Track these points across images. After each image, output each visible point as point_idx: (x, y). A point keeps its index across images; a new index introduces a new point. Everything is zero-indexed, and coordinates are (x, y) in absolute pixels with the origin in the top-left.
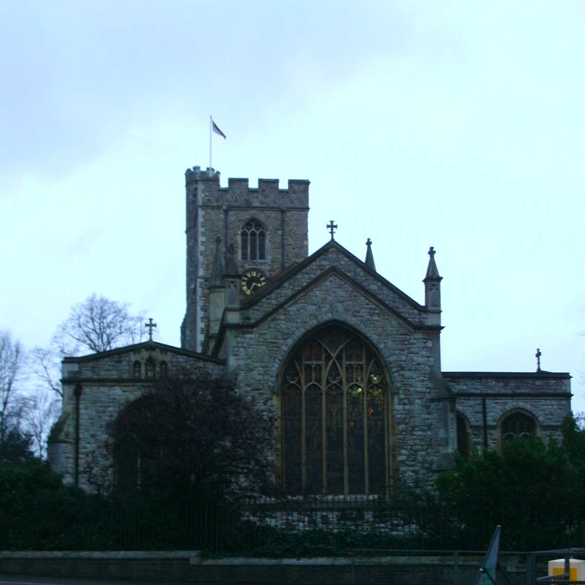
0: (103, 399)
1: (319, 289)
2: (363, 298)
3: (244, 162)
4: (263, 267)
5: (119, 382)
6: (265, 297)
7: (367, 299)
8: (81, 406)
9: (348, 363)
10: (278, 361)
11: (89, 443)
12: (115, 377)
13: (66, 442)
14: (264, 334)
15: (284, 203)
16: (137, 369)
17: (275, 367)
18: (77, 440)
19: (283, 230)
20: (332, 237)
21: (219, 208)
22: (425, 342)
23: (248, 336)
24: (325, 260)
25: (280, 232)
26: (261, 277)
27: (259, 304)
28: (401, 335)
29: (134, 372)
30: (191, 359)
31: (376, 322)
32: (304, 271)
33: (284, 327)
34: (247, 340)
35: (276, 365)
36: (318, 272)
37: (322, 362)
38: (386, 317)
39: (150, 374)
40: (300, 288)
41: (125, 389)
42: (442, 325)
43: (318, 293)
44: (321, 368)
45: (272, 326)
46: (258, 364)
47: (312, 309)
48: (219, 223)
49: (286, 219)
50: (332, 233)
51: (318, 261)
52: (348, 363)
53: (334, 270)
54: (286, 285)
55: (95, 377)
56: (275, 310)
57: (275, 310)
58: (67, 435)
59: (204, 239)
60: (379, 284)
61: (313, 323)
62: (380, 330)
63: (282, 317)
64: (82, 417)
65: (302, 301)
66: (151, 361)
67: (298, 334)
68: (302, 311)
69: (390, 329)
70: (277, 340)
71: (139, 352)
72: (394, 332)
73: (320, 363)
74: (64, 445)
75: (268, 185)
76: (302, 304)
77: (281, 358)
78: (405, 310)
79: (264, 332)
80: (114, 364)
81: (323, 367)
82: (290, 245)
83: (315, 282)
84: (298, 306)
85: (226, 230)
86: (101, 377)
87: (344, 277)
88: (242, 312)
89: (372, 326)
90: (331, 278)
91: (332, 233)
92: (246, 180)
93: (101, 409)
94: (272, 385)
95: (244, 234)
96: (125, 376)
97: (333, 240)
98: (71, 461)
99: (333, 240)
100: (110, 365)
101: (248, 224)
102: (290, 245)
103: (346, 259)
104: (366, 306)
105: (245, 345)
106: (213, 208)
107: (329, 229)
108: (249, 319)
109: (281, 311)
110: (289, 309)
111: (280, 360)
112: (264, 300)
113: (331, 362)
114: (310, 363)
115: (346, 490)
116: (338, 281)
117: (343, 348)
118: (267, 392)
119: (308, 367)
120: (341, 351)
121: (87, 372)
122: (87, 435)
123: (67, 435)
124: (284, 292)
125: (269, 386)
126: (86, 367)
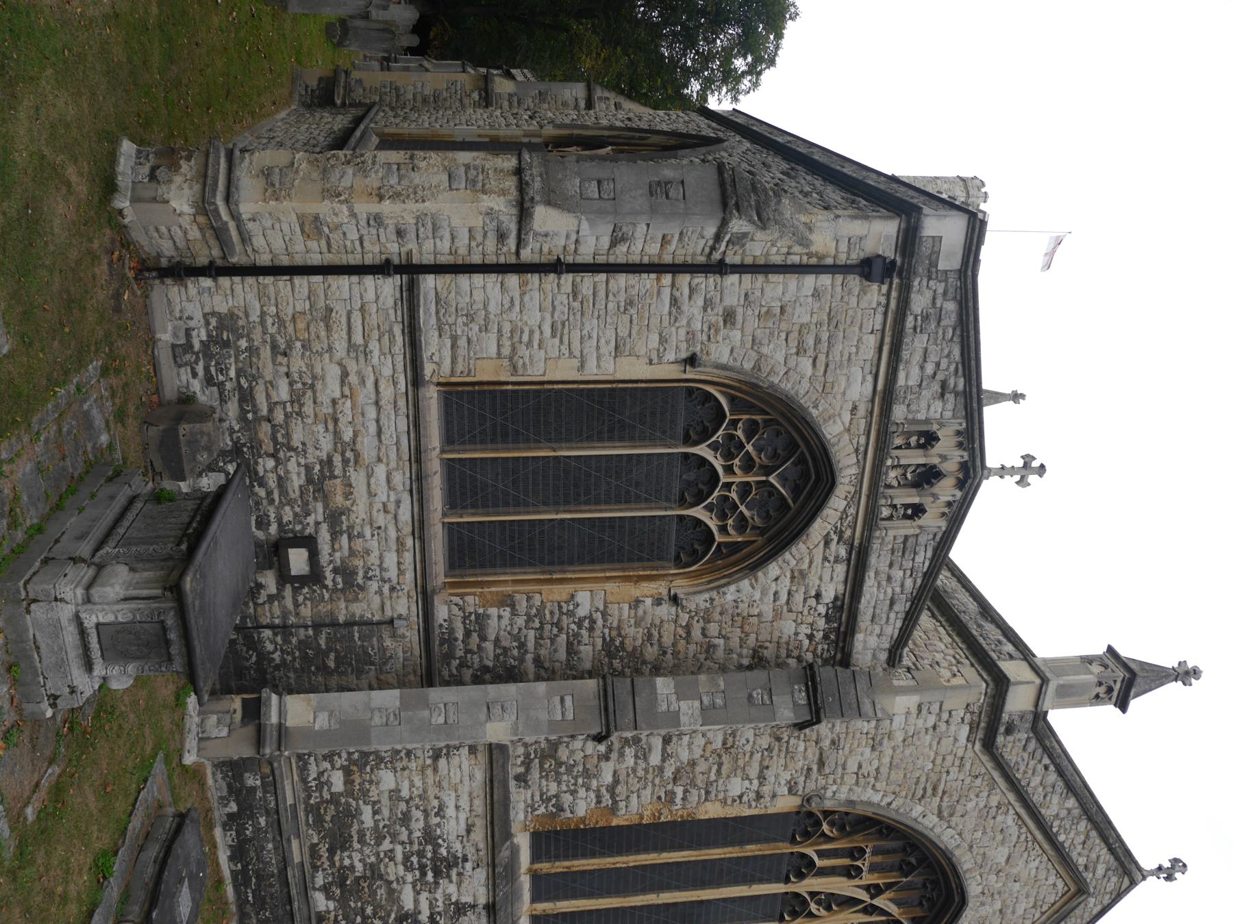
0: (838, 347)
5: (887, 397)
6: (1053, 762)
8: (826, 279)
10: (888, 800)
11: (708, 304)
12: (901, 381)
13: (718, 238)
14: (961, 766)
17: (872, 797)
18: (721, 268)
24: (1108, 870)
27: (1040, 751)
29: (908, 435)
30: (919, 581)
32: (1094, 834)
33: (970, 805)
34: (953, 728)
35: (876, 798)
36: (1082, 861)
37: (868, 879)
41: (862, 411)
44: (850, 876)
46: (886, 760)
53: (1081, 889)
54: (1071, 802)
56: (1014, 785)
57: (1014, 785)
58: (740, 239)
63: (994, 801)
64: (792, 280)
65: (1023, 836)
66: (927, 476)
67: (946, 837)
68: (999, 837)
71: (960, 445)
74: (711, 231)
76: (1014, 839)
77: (894, 806)
79: (968, 766)
80: (940, 376)
81: (857, 882)
84: (1014, 830)
88: (1031, 717)
90: (1060, 884)
93: (810, 341)
94: (829, 794)
98: (654, 249)
100: (938, 364)
105: (943, 726)
108: (1009, 731)
109: (1011, 797)
110: (1011, 812)
111: (890, 804)
112: (1046, 761)
113: (863, 895)
115: (544, 867)
117: (890, 915)
120: (883, 912)
121: (929, 294)
122: (732, 300)
123: (740, 239)
124: (1056, 799)
125: (825, 788)
126: (945, 293)
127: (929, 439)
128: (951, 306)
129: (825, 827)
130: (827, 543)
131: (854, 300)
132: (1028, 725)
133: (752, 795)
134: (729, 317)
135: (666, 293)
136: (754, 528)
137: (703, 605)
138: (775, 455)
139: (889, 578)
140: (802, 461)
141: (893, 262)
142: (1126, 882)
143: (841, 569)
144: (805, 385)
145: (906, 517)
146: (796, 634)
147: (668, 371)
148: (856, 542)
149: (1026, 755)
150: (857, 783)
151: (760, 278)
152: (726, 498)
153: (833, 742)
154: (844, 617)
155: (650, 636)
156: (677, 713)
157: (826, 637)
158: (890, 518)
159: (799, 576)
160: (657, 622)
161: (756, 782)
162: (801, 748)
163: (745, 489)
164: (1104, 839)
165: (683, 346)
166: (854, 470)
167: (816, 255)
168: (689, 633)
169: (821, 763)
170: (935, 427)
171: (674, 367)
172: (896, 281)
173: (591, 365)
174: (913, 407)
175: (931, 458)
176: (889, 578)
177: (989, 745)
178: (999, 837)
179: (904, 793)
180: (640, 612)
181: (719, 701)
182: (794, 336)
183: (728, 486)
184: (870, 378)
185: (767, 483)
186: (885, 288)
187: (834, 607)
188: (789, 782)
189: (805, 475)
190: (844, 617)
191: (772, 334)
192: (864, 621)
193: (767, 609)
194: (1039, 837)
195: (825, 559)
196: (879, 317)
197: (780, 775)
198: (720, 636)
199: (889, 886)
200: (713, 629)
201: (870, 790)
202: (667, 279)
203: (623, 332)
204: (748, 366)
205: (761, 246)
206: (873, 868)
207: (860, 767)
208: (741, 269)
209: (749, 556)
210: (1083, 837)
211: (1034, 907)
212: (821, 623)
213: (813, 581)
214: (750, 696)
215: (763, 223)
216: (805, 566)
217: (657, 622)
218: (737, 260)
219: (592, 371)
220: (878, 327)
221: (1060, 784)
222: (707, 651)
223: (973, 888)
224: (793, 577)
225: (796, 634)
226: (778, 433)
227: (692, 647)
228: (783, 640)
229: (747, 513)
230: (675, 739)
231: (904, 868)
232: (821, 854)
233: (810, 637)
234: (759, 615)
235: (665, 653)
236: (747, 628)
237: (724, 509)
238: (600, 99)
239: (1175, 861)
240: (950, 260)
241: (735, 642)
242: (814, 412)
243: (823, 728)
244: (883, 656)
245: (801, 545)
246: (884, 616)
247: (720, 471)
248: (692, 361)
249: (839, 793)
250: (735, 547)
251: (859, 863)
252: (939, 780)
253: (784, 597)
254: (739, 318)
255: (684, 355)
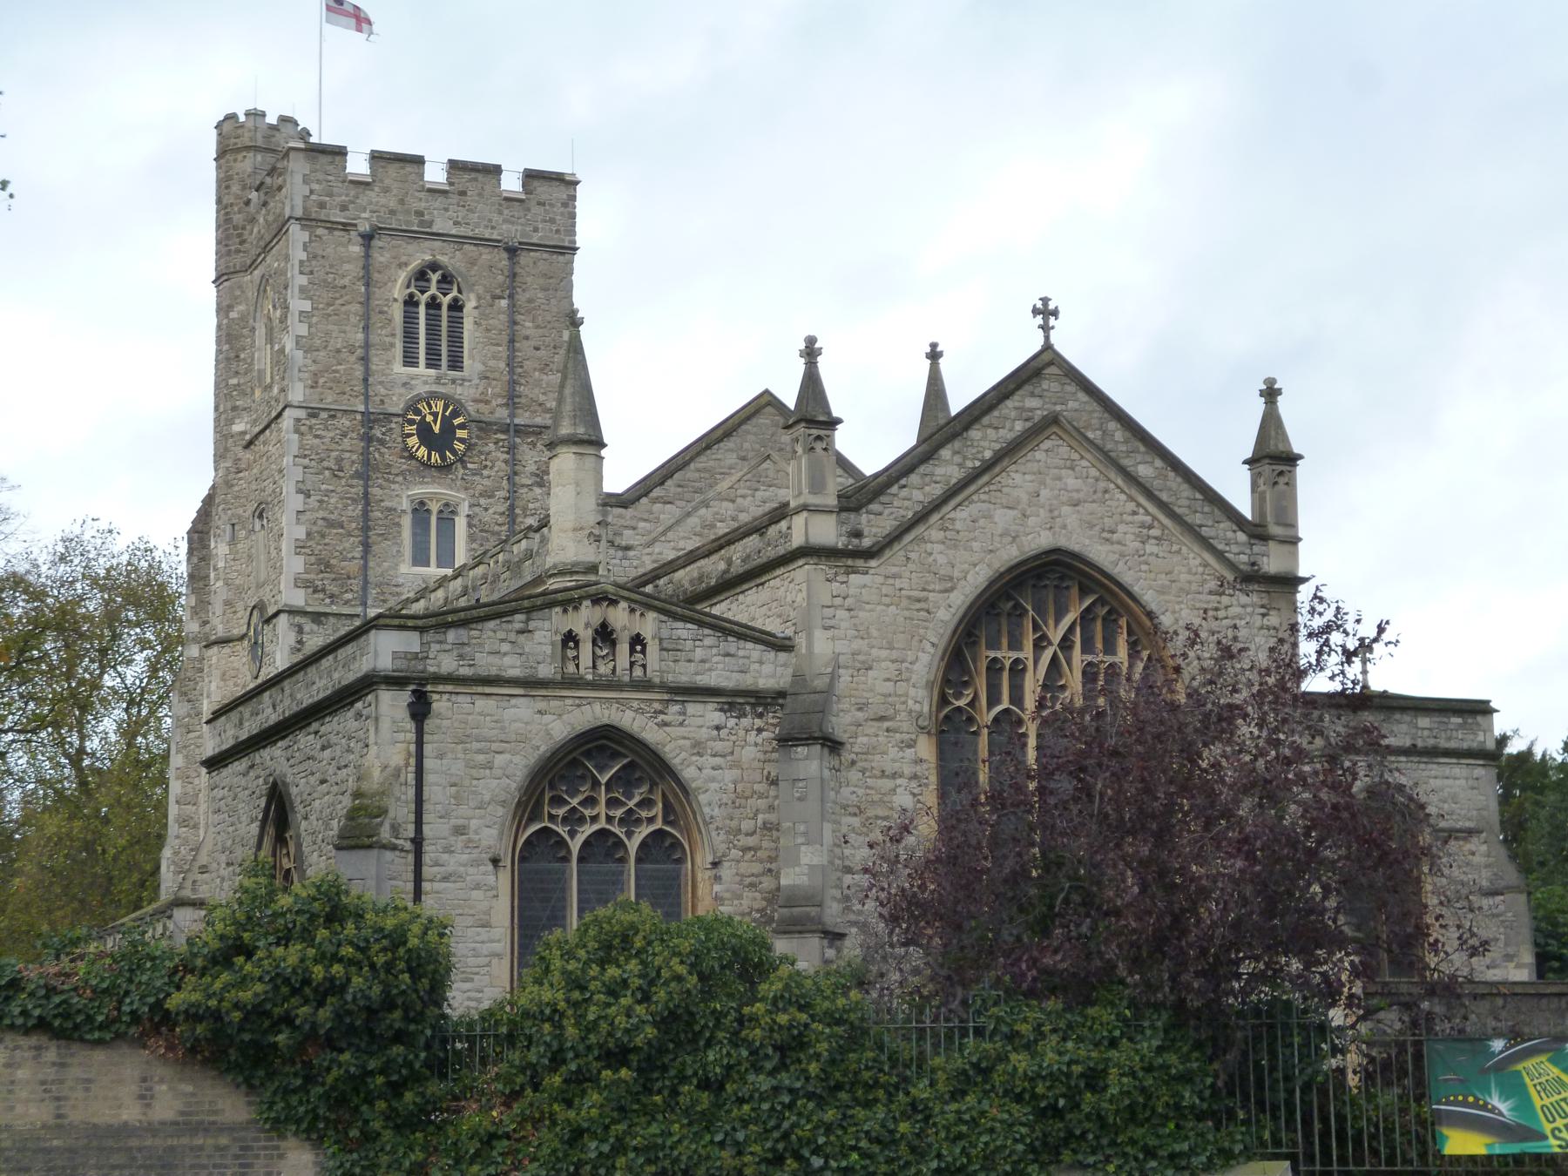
1: (1022, 468)
2: (1123, 497)
3: (364, 106)
4: (459, 390)
5: (531, 684)
6: (898, 479)
7: (1131, 498)
8: (428, 749)
9: (1090, 658)
10: (928, 647)
11: (448, 850)
13: (394, 848)
14: (894, 576)
15: (511, 231)
16: (571, 653)
17: (925, 663)
18: (418, 842)
19: (511, 296)
20: (1047, 338)
21: (346, 227)
22: (1264, 615)
23: (854, 579)
24: (1032, 395)
25: (504, 303)
26: (455, 414)
27: (883, 499)
28: (1211, 593)
29: (564, 658)
30: (707, 631)
31: (1152, 559)
32: (986, 420)
33: (942, 559)
34: (852, 591)
35: (925, 658)
36: (1019, 426)
37: (1027, 652)
38: (1175, 548)
39: (604, 669)
40: (978, 464)
41: (542, 705)
42: (1302, 573)
43: (1018, 479)
44: (1024, 670)
45: (913, 555)
46: (884, 653)
47: (1003, 518)
48: (346, 267)
49: (518, 270)
50: (1046, 328)
51: (1016, 397)
52: (1090, 658)
53: (1053, 421)
54: (945, 453)
55: (465, 671)
56: (921, 518)
57: (921, 518)
59: (307, 306)
60: (1159, 463)
61: (1010, 554)
62: (1163, 580)
63: (936, 534)
64: (429, 778)
65: (983, 497)
66: (604, 634)
69: (1184, 577)
70: (925, 594)
71: (576, 608)
72: (1194, 587)
73: (1021, 655)
75: (473, 175)
78: (1222, 532)
80: (512, 637)
81: (1030, 664)
82: (527, 338)
83: (1011, 451)
85: (367, 285)
86: (483, 672)
87: (1079, 437)
88: (844, 515)
89: (1144, 567)
90: (1047, 444)
91: (1046, 328)
92: (418, 161)
94: (917, 707)
95: (411, 302)
96: (546, 671)
97: (1048, 347)
99: (1048, 347)
100: (503, 640)
101: (421, 276)
102: (527, 338)
103: (1082, 396)
104: (1130, 518)
105: (849, 602)
106: (332, 226)
107: (1039, 320)
108: (858, 534)
109: (935, 517)
110: (952, 515)
111: (933, 645)
112: (894, 489)
114: (999, 655)
116: (1064, 450)
117: (1074, 624)
118: (905, 724)
119: (994, 667)
120: (1071, 629)
121: (442, 656)
123: (395, 829)
124: (939, 471)
126: (440, 642)
127: (570, 638)
128: (451, 635)
129: (962, 703)
130: (665, 724)
131: (446, 723)
132: (852, 516)
133: (914, 784)
134: (459, 831)
135: (437, 886)
136: (651, 791)
137: (722, 837)
138: (583, 777)
139: (703, 661)
140: (588, 754)
141: (414, 692)
142: (1053, 370)
143: (692, 708)
144: (517, 759)
145: (643, 652)
146: (756, 744)
147: (504, 881)
148: (666, 697)
149: (887, 512)
150: (907, 680)
151: (426, 806)
152: (621, 820)
153: (860, 709)
154: (738, 700)
155: (752, 885)
156: (811, 867)
157: (761, 716)
158: (644, 666)
159: (698, 748)
160: (738, 878)
161: (899, 781)
162: (865, 740)
163: (612, 803)
164: (991, 408)
165: (482, 868)
166: (597, 707)
167: (407, 760)
168: (750, 849)
169: (882, 719)
170: (559, 638)
171: (500, 875)
172: (429, 688)
173: (498, 947)
174: (540, 658)
175: (585, 635)
176: (703, 661)
177: (869, 554)
178: (982, 522)
179: (922, 631)
180: (727, 895)
181: (802, 828)
182: (474, 772)
183: (609, 819)
184: (514, 701)
185: (608, 784)
186: (435, 697)
187: (730, 710)
188: (901, 749)
189: (601, 749)
190: (738, 700)
191: (474, 793)
192: (747, 681)
193: (729, 775)
194: (985, 478)
195: (681, 724)
196: (460, 698)
197: (893, 757)
198: (755, 817)
199: (1036, 627)
200: (747, 825)
201: (915, 667)
202: (426, 886)
203: (470, 921)
204: (500, 811)
205: (402, 811)
206: (1015, 645)
207: (888, 680)
208: (419, 823)
209: (676, 795)
210: (989, 431)
211: (1072, 469)
212: (745, 722)
213: (704, 733)
214: (799, 799)
215: (383, 812)
216: (687, 743)
217: (738, 878)
218: (411, 827)
219: (503, 946)
220: (468, 699)
221: (922, 469)
222: (770, 830)
223: (1042, 540)
224: (699, 754)
225: (756, 744)
226: (563, 777)
227: (765, 844)
228: (762, 757)
229: (637, 799)
230: (847, 863)
231: (1019, 612)
232: (993, 700)
233: (760, 730)
234: (735, 782)
235: (770, 870)
236: (748, 793)
237: (630, 820)
238: (194, 890)
239: (1036, 312)
240: (409, 642)
241: (762, 803)
242: (543, 749)
243: (841, 723)
244: (783, 656)
245: (667, 749)
246: (741, 661)
247: (596, 827)
248: (495, 861)
249: (919, 698)
250: (668, 808)
251: (1007, 664)
252: (909, 598)
253: (718, 760)
254: (460, 822)
255: (490, 867)
